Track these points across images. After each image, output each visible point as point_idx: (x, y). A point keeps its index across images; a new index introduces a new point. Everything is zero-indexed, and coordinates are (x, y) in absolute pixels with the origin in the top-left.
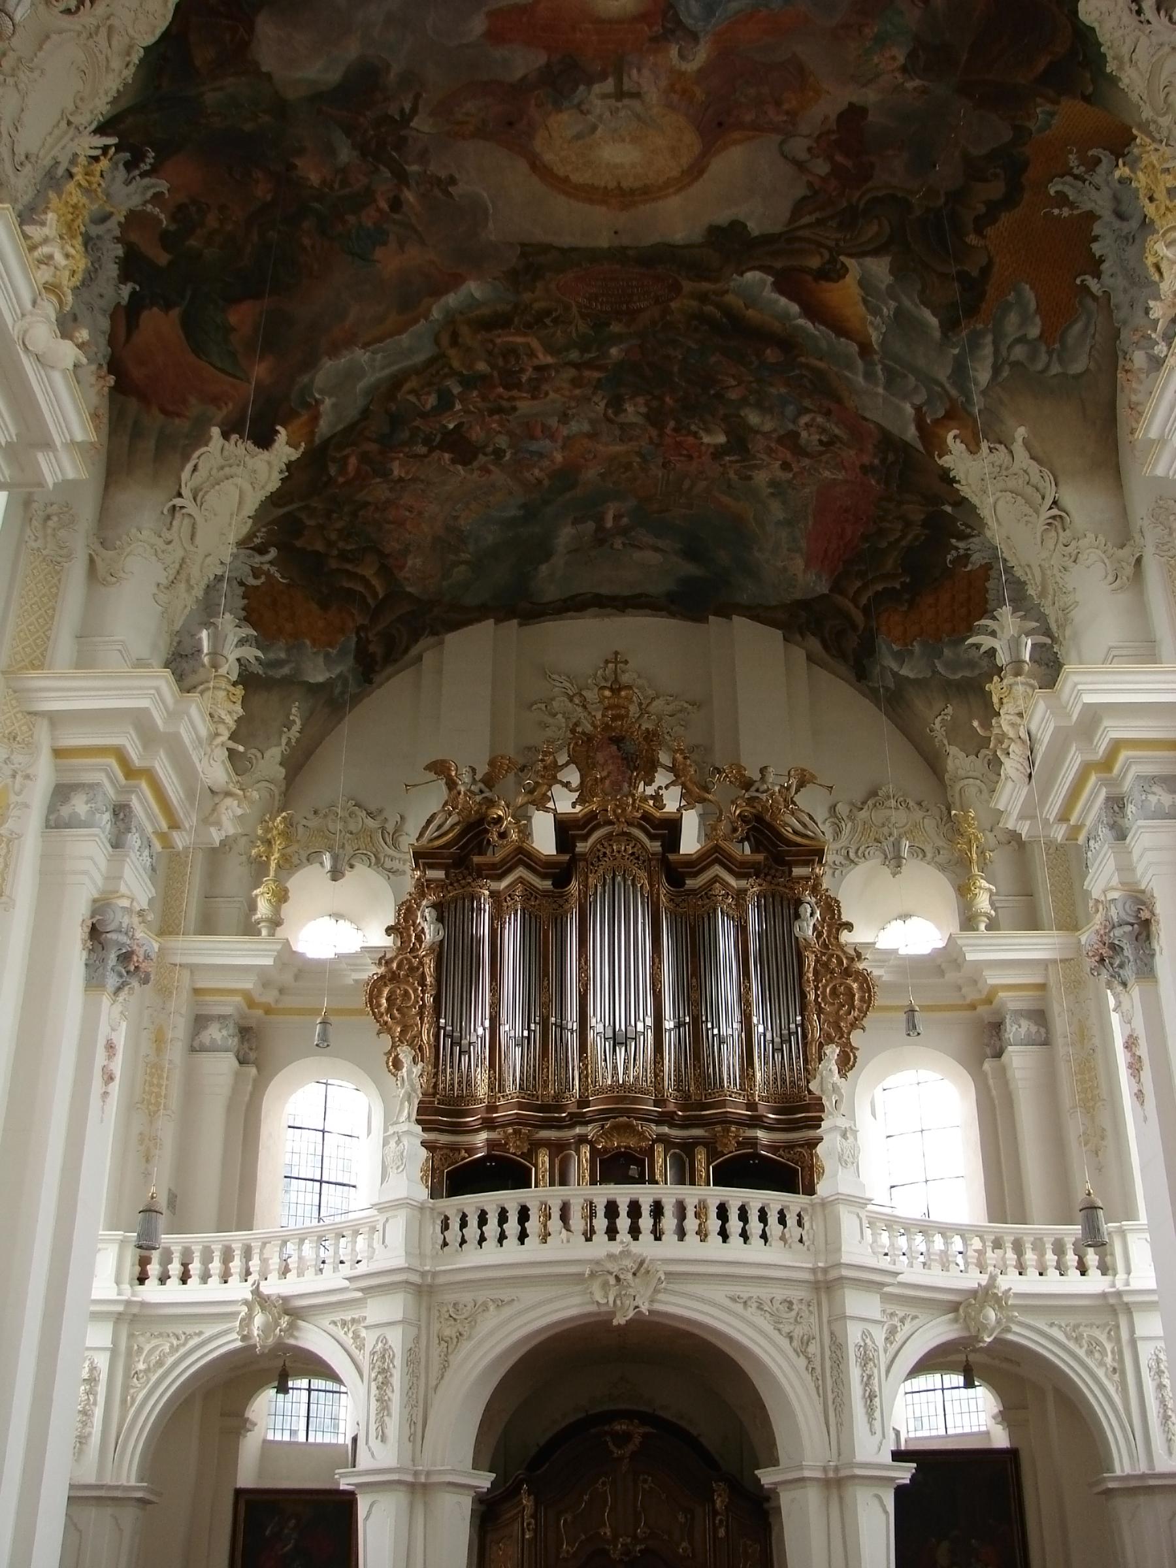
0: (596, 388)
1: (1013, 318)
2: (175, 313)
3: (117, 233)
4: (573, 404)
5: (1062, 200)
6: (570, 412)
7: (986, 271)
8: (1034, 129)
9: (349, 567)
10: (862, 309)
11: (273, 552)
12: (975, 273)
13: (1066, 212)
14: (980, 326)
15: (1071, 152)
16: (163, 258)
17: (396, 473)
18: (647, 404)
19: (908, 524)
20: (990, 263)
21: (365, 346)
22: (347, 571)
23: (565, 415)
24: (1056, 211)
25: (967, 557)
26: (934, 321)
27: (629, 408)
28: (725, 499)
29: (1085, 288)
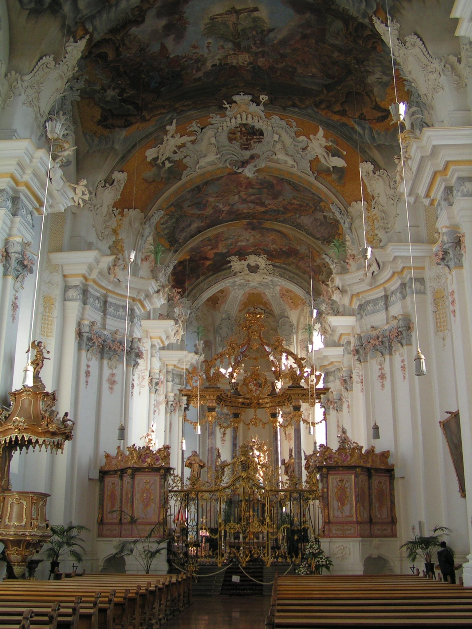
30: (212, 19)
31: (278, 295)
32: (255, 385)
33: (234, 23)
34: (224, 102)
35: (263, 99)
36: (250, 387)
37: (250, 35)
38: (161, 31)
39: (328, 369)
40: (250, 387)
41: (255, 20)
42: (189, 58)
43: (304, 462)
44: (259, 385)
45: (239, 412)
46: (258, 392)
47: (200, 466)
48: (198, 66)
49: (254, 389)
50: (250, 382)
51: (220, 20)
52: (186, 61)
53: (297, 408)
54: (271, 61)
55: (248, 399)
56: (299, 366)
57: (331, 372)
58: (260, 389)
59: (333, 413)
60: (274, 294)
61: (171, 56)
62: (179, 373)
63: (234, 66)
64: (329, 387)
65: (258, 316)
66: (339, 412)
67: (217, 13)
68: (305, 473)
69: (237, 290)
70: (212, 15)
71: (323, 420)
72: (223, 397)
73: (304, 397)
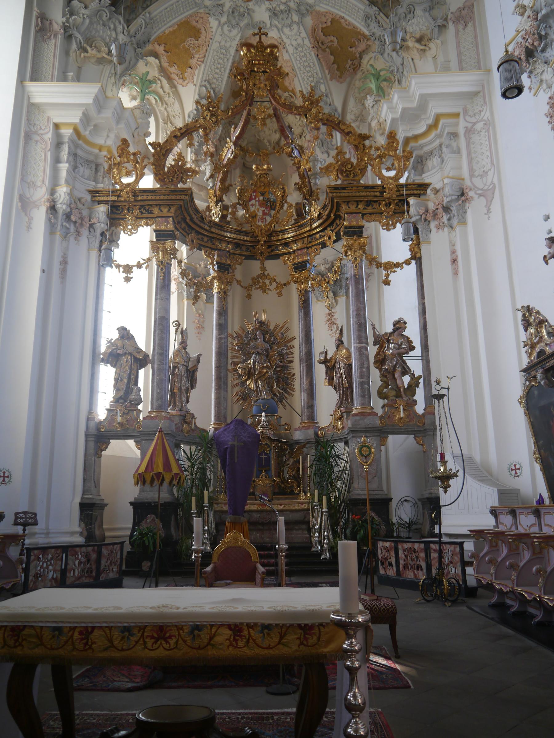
31: (307, 42)
32: (261, 205)
36: (252, 209)
39: (422, 147)
40: (252, 209)
43: (372, 351)
44: (270, 205)
45: (229, 262)
46: (269, 219)
47: (136, 359)
49: (260, 214)
50: (251, 199)
53: (356, 232)
55: (246, 233)
56: (356, 148)
57: (431, 153)
58: (273, 212)
59: (437, 242)
60: (300, 41)
62: (91, 158)
64: (427, 181)
65: (268, 50)
66: (458, 229)
68: (375, 375)
69: (226, 28)
71: (411, 259)
72: (192, 219)
73: (370, 209)
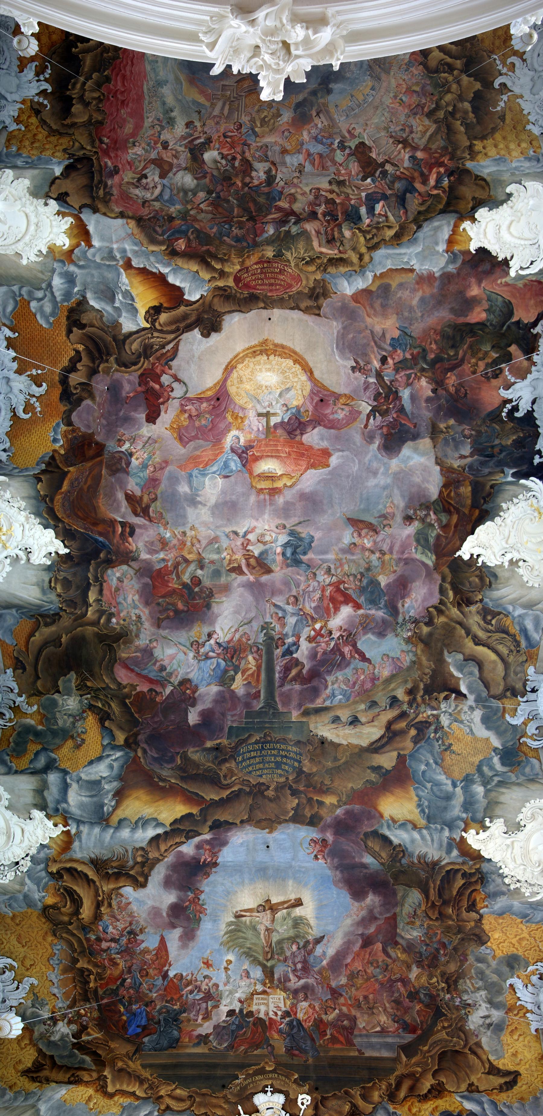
0: (281, 193)
1: (48, 308)
2: (515, 319)
3: (533, 368)
4: (295, 181)
5: (37, 381)
6: (298, 174)
7: (69, 332)
8: (62, 426)
9: (449, 60)
10: (134, 293)
11: (496, 85)
12: (75, 329)
13: (34, 372)
14: (66, 304)
15: (40, 412)
16: (513, 349)
17: (407, 157)
18: (252, 178)
19: (81, 99)
20: (68, 336)
21: (412, 270)
22: (451, 57)
23: (300, 172)
24: (39, 372)
25: (37, 74)
26: (92, 303)
27: (263, 176)
28: (202, 100)
29: (12, 329)
30: (238, 916)
33: (267, 929)
34: (240, 1108)
35: (303, 1104)
37: (288, 954)
38: (165, 914)
41: (298, 922)
42: (196, 987)
48: (207, 1008)
51: (247, 920)
52: (191, 992)
54: (317, 1009)
61: (171, 974)
63: (261, 1019)
67: (246, 907)
70: (239, 909)
